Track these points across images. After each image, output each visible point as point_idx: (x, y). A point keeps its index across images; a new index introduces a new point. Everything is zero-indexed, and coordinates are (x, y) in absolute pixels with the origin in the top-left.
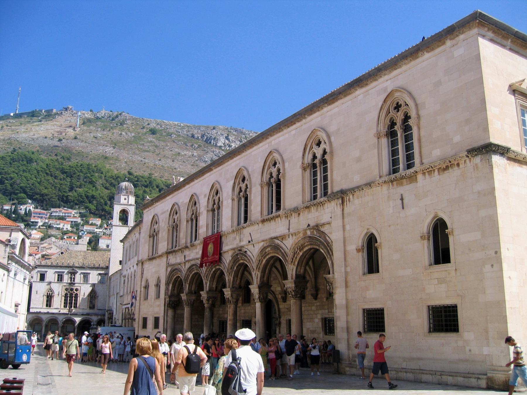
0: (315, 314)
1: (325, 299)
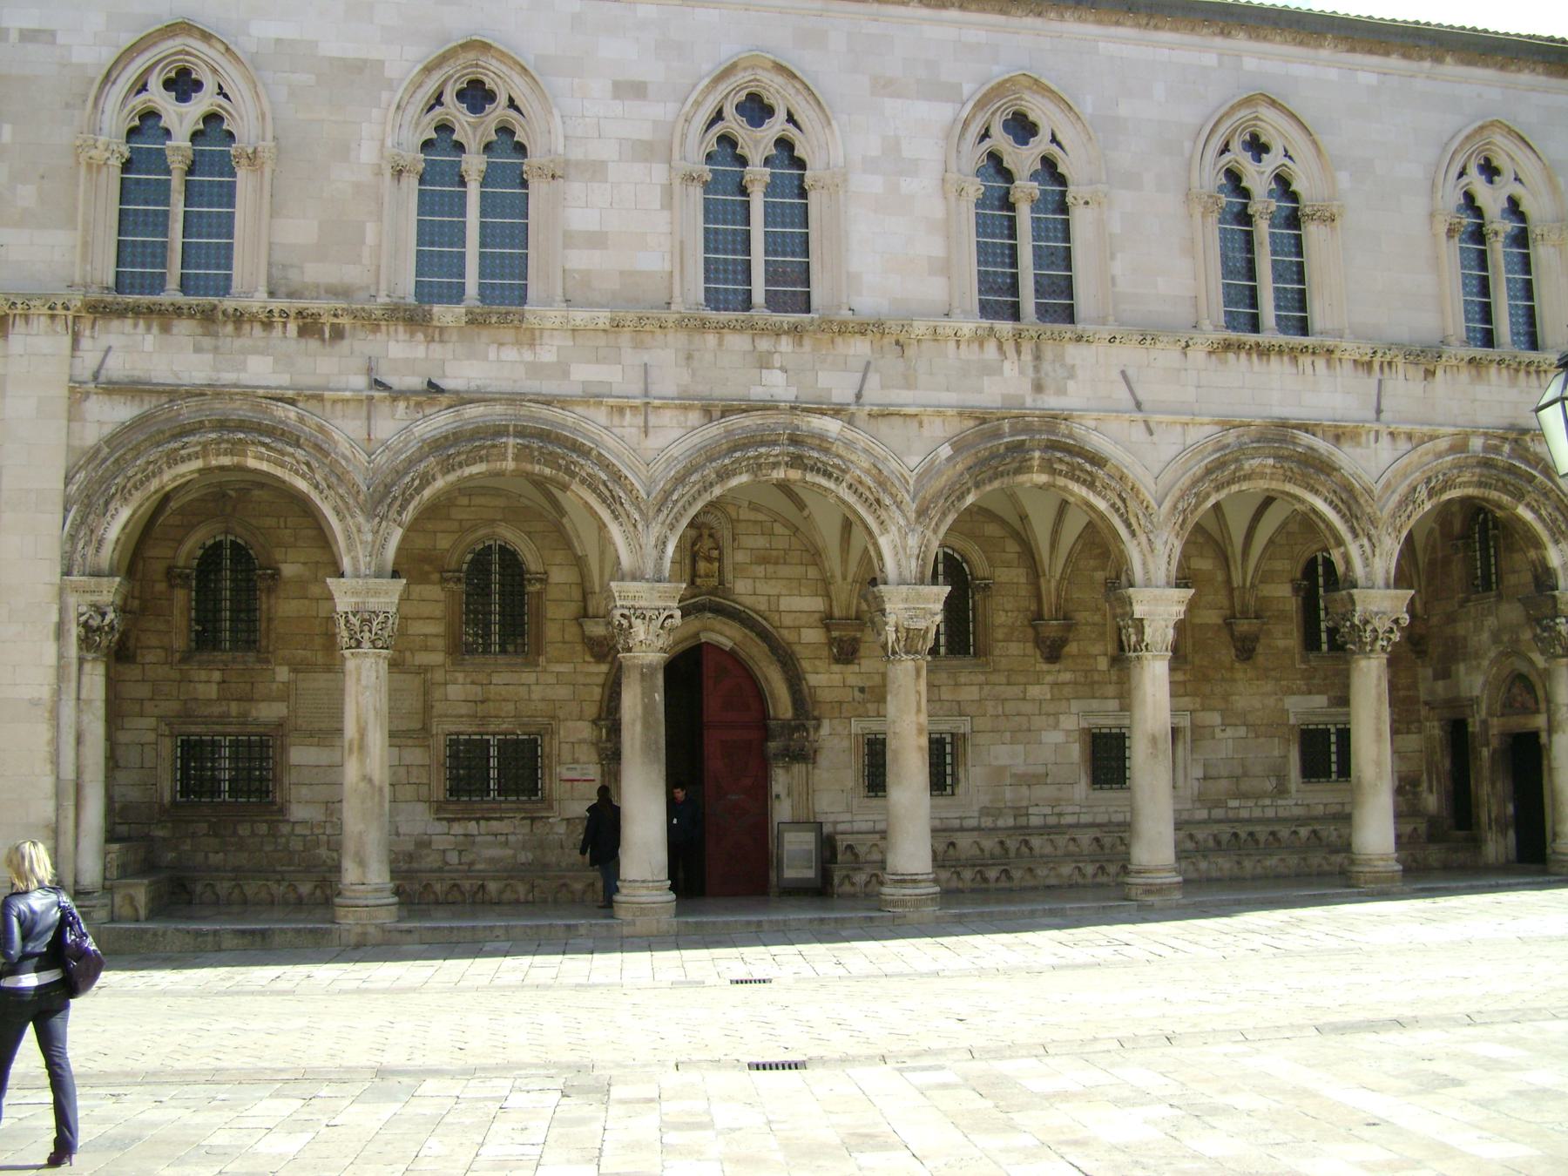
0: (1048, 715)
1: (1103, 663)
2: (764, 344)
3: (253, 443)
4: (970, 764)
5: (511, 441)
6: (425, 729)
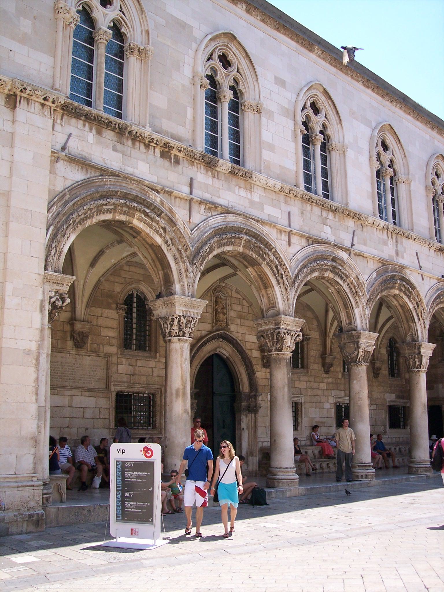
0: (326, 396)
2: (325, 214)
3: (140, 211)
4: (303, 416)
5: (246, 237)
6: (107, 387)
